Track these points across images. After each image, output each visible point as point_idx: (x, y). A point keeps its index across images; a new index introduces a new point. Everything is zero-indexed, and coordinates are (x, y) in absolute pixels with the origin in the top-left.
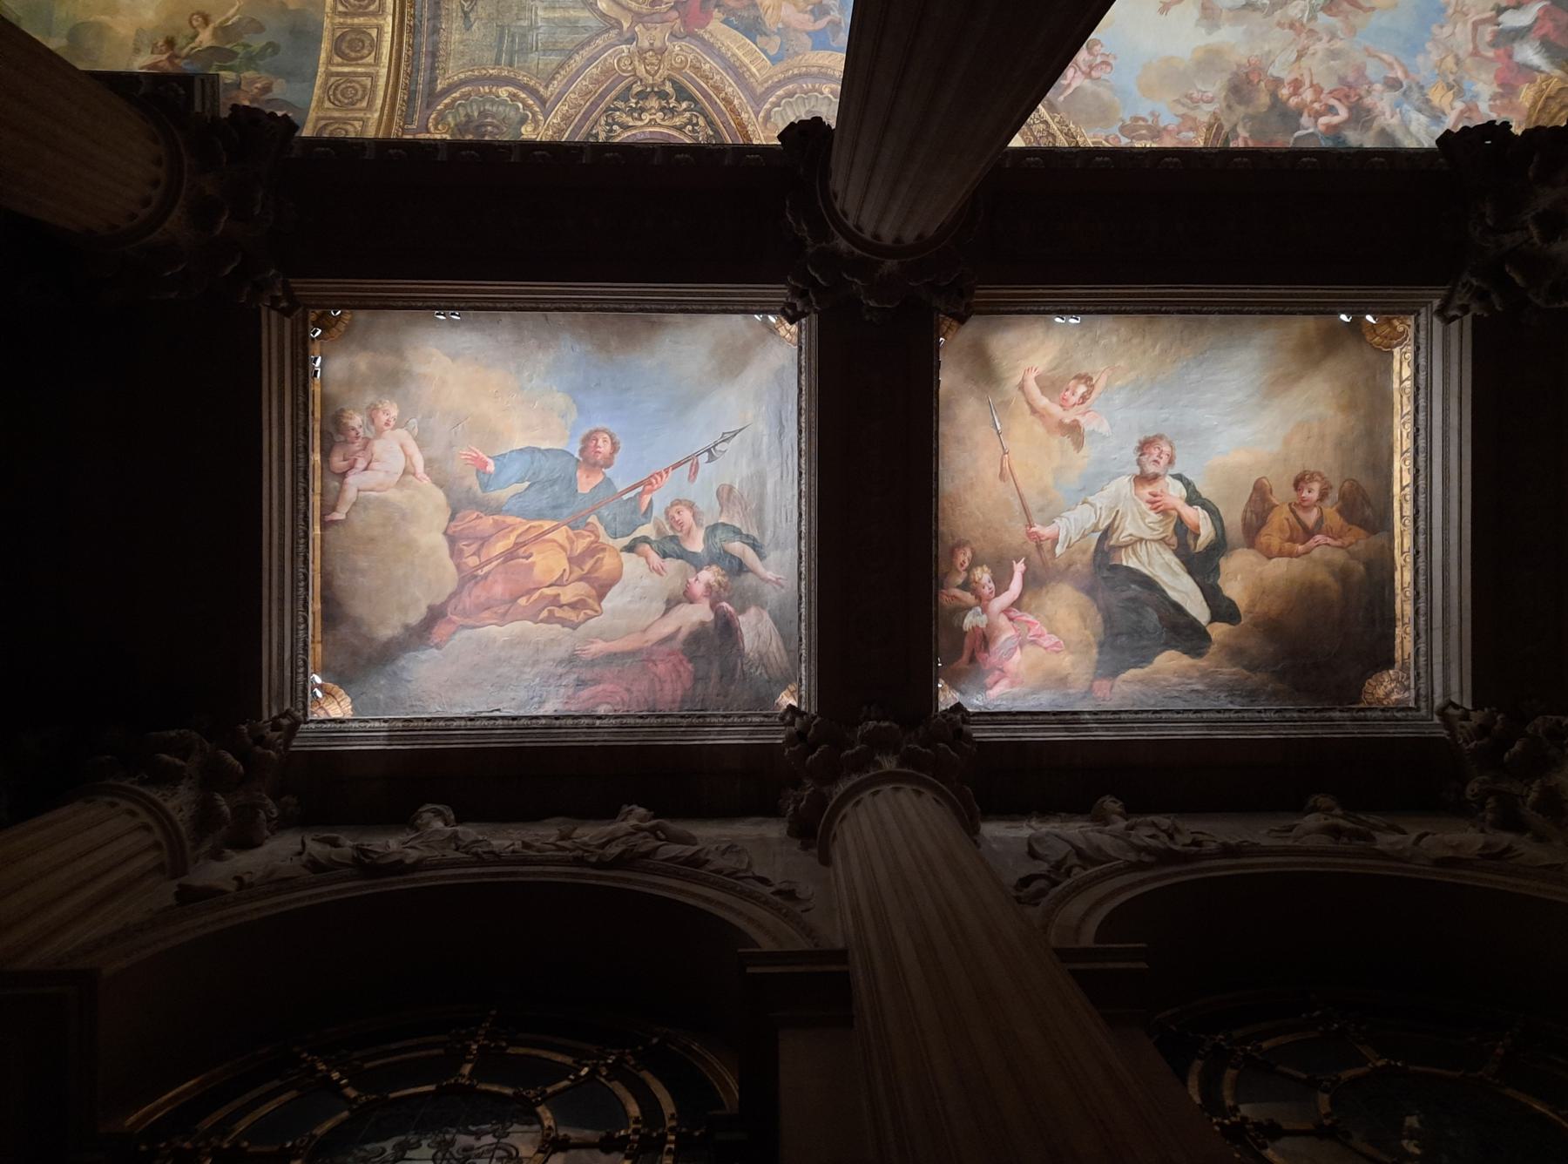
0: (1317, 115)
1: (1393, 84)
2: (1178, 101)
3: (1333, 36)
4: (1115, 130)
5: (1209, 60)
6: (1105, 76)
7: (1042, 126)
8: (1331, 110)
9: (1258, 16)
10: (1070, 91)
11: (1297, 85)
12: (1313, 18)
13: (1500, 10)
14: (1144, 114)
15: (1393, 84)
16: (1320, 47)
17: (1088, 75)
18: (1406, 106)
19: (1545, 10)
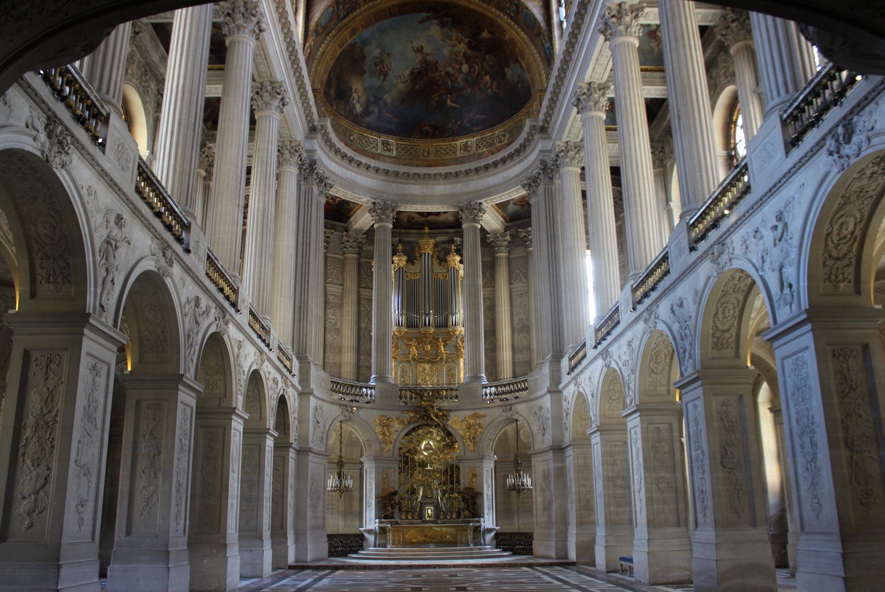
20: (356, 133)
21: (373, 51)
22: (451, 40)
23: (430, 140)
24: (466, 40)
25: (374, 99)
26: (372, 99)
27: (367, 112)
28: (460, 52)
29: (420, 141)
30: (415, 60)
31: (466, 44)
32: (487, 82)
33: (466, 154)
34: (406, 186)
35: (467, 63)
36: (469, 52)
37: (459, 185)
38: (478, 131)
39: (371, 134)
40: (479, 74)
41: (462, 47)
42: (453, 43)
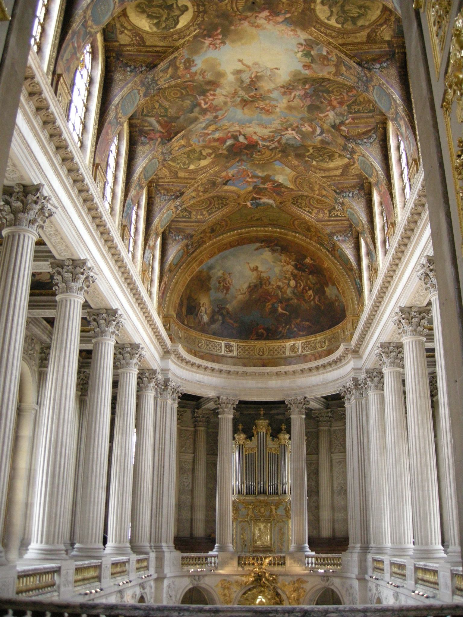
0: (204, 100)
1: (216, 117)
2: (202, 69)
3: (232, 102)
4: (187, 57)
5: (220, 75)
6: (210, 49)
7: (188, 33)
8: (206, 103)
9: (239, 84)
10: (203, 40)
11: (214, 95)
12: (239, 97)
13: (244, 135)
14: (195, 63)
15: (216, 117)
16: (228, 99)
17: (210, 44)
18: (207, 122)
19: (245, 144)
20: (203, 338)
21: (218, 273)
22: (281, 262)
23: (264, 342)
24: (293, 263)
25: (219, 310)
26: (217, 309)
27: (213, 320)
28: (288, 271)
29: (256, 342)
30: (252, 277)
31: (293, 266)
32: (311, 295)
33: (293, 354)
34: (244, 381)
35: (294, 279)
36: (296, 271)
37: (288, 381)
38: (304, 336)
39: (216, 339)
40: (303, 289)
41: (290, 268)
42: (282, 264)
